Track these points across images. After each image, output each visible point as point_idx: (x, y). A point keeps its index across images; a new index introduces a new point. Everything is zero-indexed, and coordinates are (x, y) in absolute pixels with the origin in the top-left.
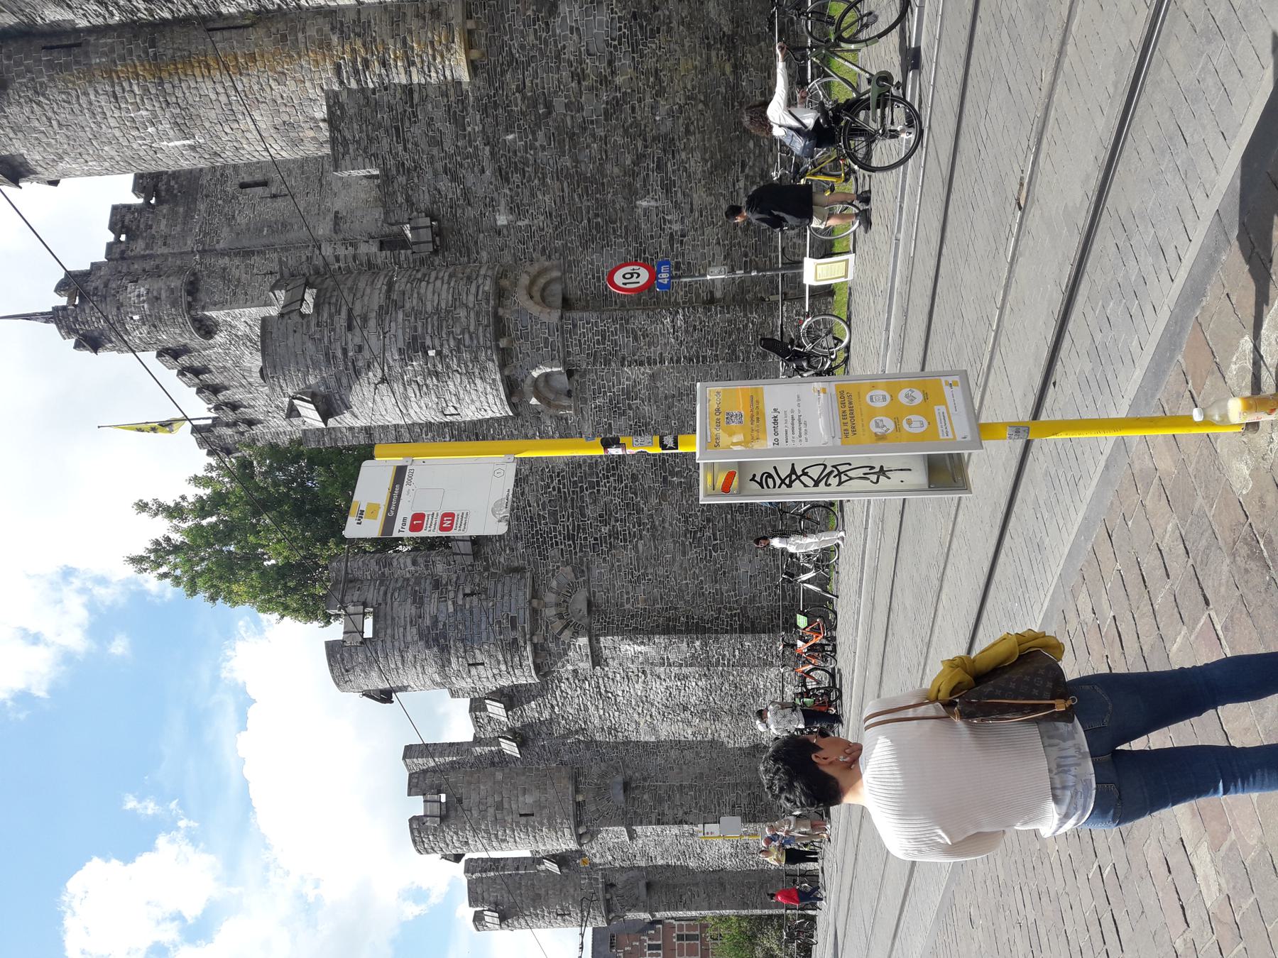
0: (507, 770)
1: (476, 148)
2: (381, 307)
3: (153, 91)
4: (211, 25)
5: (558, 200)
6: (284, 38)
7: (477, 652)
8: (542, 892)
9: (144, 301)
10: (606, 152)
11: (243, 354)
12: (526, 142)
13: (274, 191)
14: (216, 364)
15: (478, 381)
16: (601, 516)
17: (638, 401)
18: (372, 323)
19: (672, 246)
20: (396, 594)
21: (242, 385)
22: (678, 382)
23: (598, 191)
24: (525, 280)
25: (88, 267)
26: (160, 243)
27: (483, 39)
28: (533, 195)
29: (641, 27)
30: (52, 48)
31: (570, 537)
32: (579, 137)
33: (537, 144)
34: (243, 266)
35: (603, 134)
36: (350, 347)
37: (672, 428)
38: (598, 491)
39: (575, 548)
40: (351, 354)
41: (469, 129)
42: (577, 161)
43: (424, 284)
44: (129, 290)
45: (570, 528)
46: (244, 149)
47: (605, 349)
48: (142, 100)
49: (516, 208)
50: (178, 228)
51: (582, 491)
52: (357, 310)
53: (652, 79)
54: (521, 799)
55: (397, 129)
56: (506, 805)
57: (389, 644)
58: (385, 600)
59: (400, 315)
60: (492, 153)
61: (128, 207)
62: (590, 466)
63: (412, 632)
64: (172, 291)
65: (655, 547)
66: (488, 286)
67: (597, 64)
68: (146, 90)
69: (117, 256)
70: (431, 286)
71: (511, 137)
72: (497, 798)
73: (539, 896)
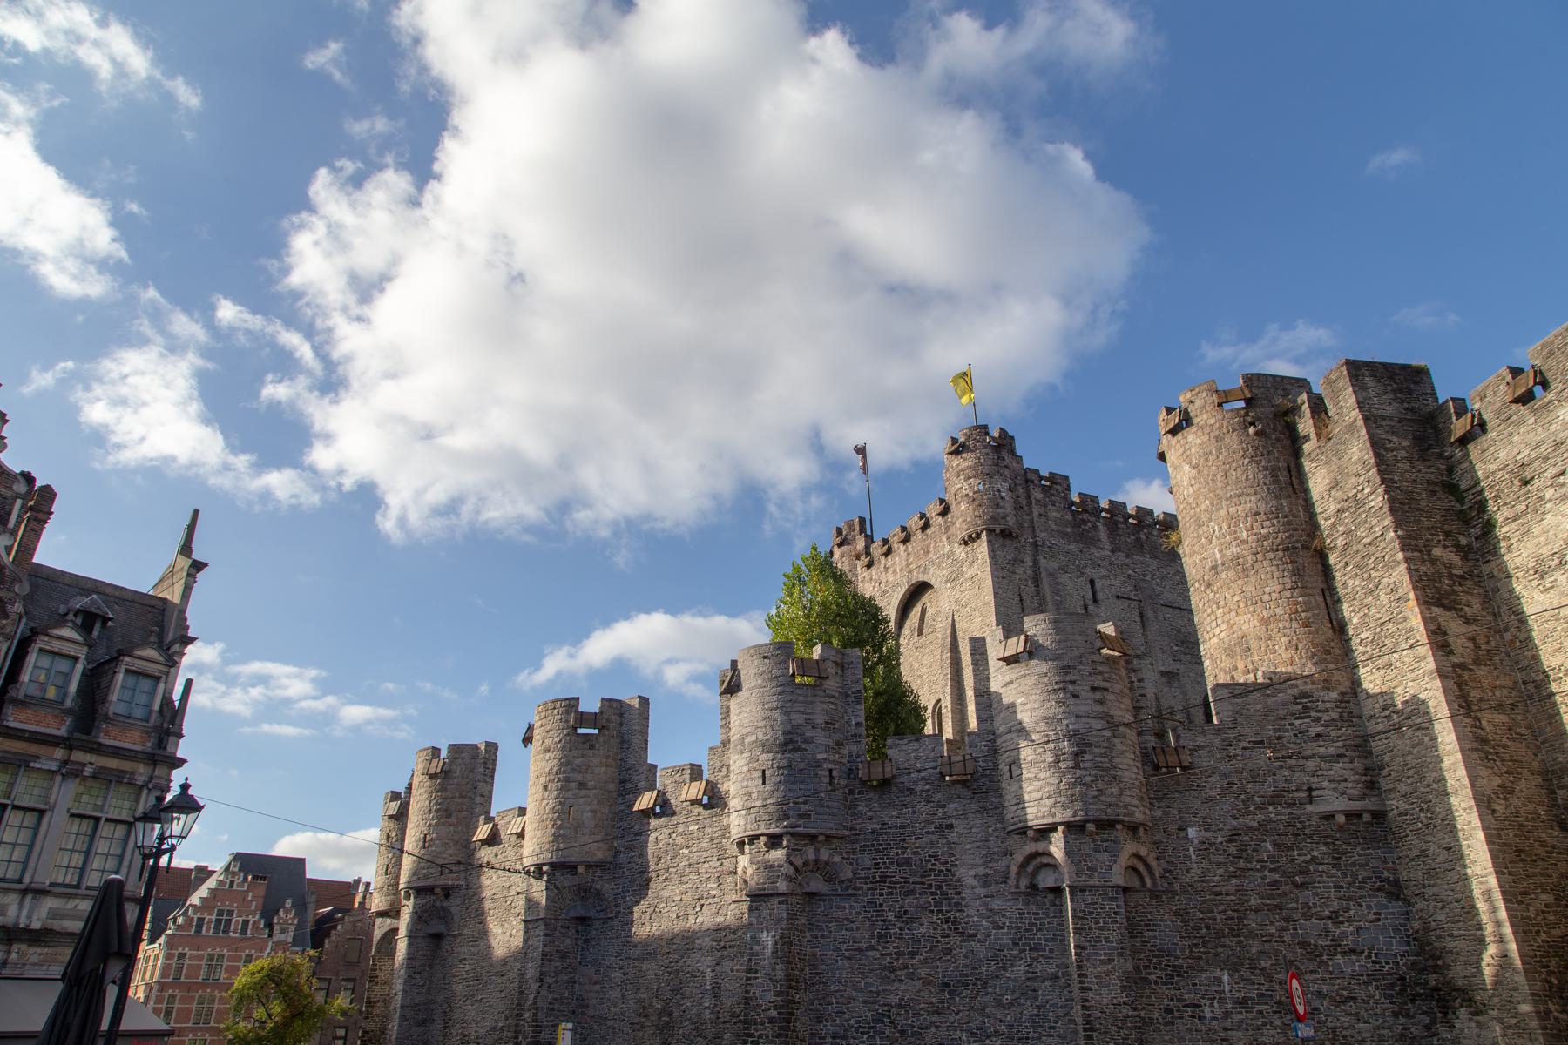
0: (615, 795)
1: (1255, 814)
4: (1327, 593)
5: (1218, 889)
6: (1328, 652)
7: (778, 779)
8: (453, 820)
9: (994, 495)
10: (1269, 941)
11: (943, 569)
12: (1266, 862)
13: (1091, 608)
16: (906, 912)
17: (1029, 960)
18: (1099, 708)
20: (832, 706)
21: (908, 565)
22: (1051, 1006)
23: (1232, 930)
24: (1143, 852)
26: (1042, 511)
27: (1354, 828)
28: (1219, 864)
29: (1392, 985)
30: (1290, 471)
31: (883, 879)
32: (1278, 914)
33: (1266, 873)
34: (1025, 576)
35: (1285, 939)
36: (1077, 688)
37: (1002, 995)
38: (933, 911)
39: (872, 882)
40: (1071, 687)
41: (1271, 808)
42: (1257, 910)
45: (893, 879)
46: (1218, 608)
47: (1091, 929)
49: (1205, 847)
50: (1054, 527)
51: (932, 894)
52: (1109, 697)
53: (1345, 993)
54: (588, 808)
55: (1262, 742)
56: (583, 792)
57: (790, 697)
58: (828, 696)
60: (1251, 828)
61: (1068, 489)
62: (957, 904)
63: (798, 719)
64: (1004, 518)
65: (872, 970)
66: (1138, 816)
67: (1350, 938)
68: (1266, 538)
69: (1029, 477)
70: (1131, 762)
71: (1269, 846)
72: (590, 784)
73: (449, 816)
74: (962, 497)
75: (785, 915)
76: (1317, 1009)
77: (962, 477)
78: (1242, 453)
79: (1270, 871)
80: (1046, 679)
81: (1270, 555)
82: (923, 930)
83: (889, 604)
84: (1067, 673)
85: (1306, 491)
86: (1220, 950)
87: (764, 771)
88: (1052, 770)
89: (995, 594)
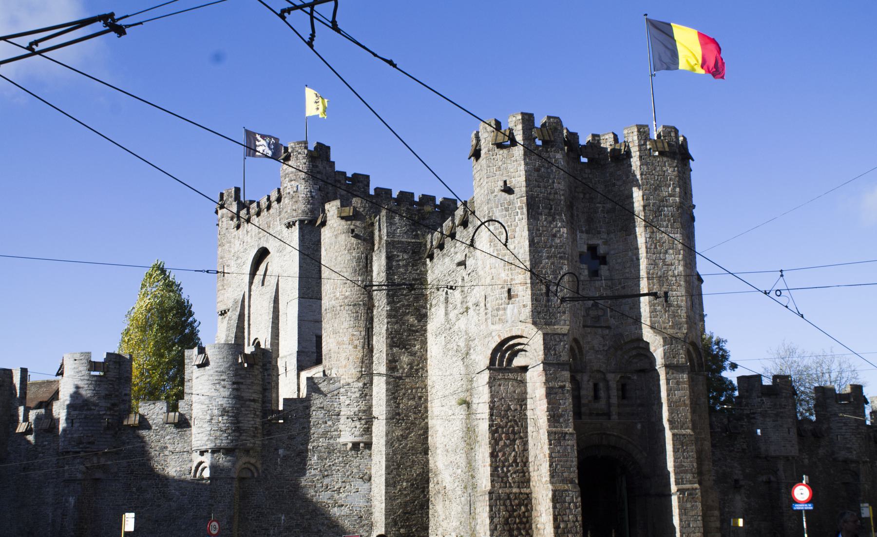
2: (242, 397)
3: (346, 301)
5: (288, 478)
14: (272, 222)
15: (207, 438)
19: (263, 529)
20: (111, 386)
24: (253, 461)
25: (332, 160)
28: (290, 467)
29: (356, 520)
40: (222, 383)
43: (253, 416)
44: (315, 186)
47: (217, 497)
48: (343, 295)
49: (285, 458)
52: (242, 387)
55: (323, 408)
58: (109, 380)
59: (238, 406)
61: (368, 185)
68: (346, 298)
70: (252, 419)
74: (286, 194)
75: (80, 490)
76: (320, 530)
77: (287, 179)
78: (345, 247)
79: (314, 469)
80: (211, 378)
81: (347, 308)
82: (148, 496)
83: (247, 259)
84: (221, 375)
85: (372, 271)
86: (283, 505)
87: (72, 420)
88: (209, 423)
89: (300, 267)
